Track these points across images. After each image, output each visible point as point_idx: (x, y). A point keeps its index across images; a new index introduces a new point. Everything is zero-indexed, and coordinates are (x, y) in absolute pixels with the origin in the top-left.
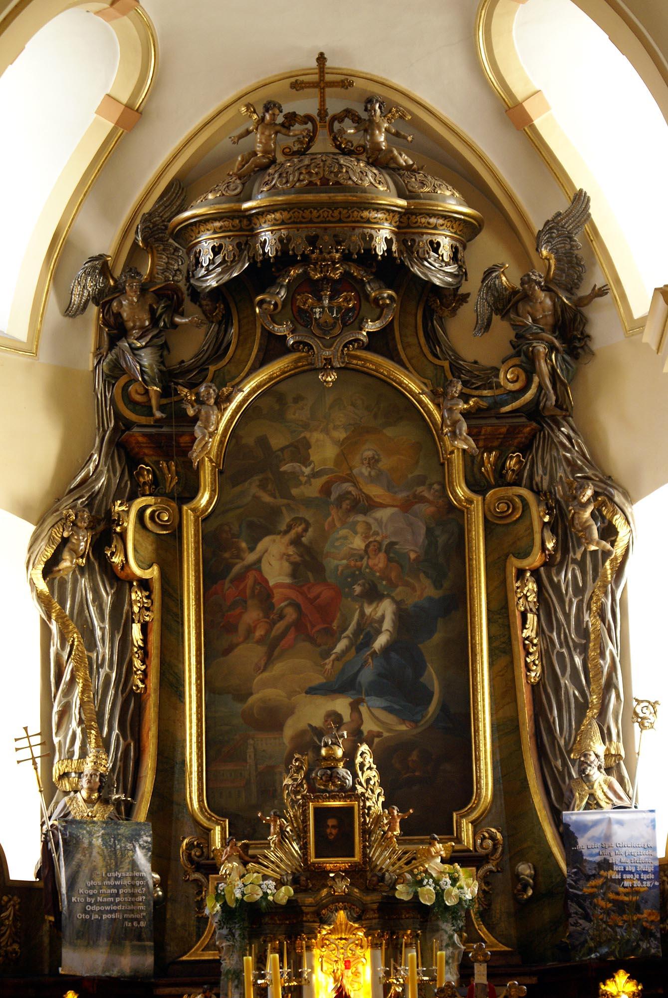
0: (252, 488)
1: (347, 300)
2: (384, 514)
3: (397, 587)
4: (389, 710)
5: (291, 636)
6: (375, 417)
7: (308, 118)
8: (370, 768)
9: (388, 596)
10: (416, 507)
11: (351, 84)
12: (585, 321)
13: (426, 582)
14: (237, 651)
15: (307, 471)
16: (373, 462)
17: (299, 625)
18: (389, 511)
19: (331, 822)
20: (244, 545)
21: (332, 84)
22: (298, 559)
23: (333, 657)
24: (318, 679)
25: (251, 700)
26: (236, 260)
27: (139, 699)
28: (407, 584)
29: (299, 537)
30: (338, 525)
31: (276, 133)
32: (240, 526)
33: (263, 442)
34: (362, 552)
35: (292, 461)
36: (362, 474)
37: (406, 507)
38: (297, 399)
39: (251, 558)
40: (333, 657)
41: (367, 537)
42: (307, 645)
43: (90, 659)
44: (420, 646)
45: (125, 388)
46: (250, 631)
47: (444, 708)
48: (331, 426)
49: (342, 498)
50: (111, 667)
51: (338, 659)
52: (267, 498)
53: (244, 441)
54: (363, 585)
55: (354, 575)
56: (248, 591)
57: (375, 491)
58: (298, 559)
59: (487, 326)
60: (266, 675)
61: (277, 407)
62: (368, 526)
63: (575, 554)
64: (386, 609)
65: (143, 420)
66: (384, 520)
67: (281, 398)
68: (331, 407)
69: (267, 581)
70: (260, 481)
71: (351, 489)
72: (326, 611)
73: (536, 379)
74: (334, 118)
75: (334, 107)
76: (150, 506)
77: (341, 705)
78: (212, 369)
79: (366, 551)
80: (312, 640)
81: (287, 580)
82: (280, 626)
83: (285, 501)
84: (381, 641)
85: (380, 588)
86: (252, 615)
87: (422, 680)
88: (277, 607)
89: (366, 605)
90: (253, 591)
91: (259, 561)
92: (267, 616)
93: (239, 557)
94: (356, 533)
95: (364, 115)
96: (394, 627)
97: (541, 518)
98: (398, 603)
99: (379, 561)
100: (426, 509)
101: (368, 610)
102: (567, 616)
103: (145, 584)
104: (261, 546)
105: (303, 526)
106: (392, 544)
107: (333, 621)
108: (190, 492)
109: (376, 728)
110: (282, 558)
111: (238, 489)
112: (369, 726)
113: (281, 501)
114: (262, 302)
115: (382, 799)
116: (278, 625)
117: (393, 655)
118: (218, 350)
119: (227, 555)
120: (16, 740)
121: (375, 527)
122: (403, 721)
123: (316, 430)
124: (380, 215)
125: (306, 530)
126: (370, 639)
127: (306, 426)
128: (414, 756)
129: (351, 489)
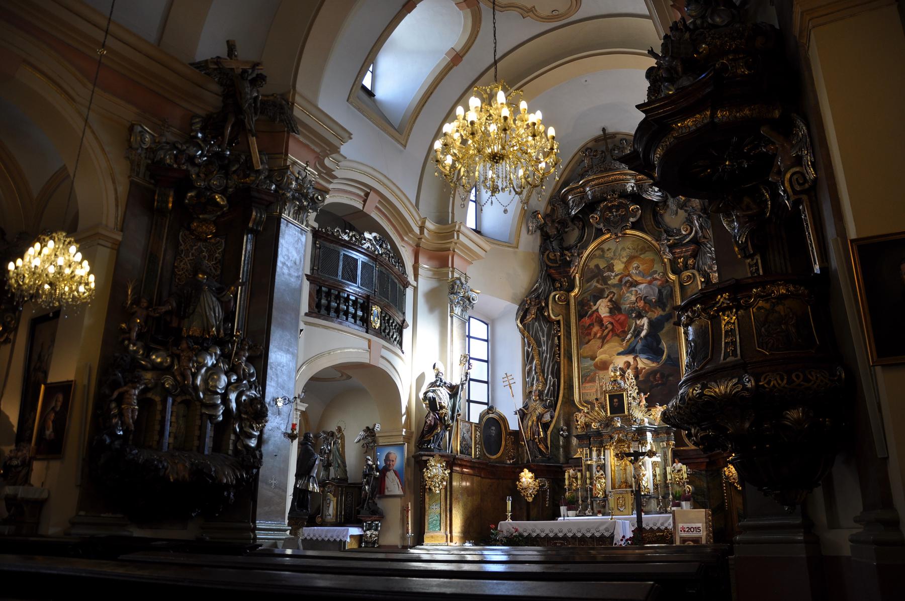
0: (594, 283)
1: (622, 212)
2: (642, 286)
3: (648, 312)
4: (648, 359)
5: (610, 334)
7: (603, 152)
8: (632, 379)
9: (646, 316)
11: (615, 137)
13: (660, 309)
14: (591, 343)
15: (613, 274)
17: (612, 330)
18: (644, 285)
19: (615, 400)
20: (592, 304)
21: (610, 138)
22: (611, 306)
24: (621, 350)
25: (596, 359)
26: (580, 203)
27: (559, 364)
29: (612, 298)
31: (592, 159)
33: (597, 266)
37: (650, 283)
38: (608, 250)
39: (594, 308)
42: (616, 337)
43: (539, 351)
44: (659, 334)
45: (548, 255)
46: (596, 334)
47: (669, 356)
49: (626, 282)
50: (547, 353)
51: (628, 341)
52: (599, 286)
55: (632, 310)
57: (639, 279)
58: (611, 306)
59: (677, 213)
60: (602, 349)
62: (637, 291)
64: (645, 321)
65: (555, 265)
67: (603, 250)
68: (621, 250)
72: (622, 324)
73: (694, 229)
74: (611, 150)
75: (610, 146)
76: (556, 295)
77: (630, 358)
78: (579, 245)
79: (636, 301)
80: (618, 335)
81: (608, 315)
82: (606, 331)
84: (643, 334)
85: (642, 314)
86: (596, 328)
87: (660, 346)
90: (596, 319)
91: (598, 309)
92: (601, 328)
95: (621, 146)
97: (701, 280)
98: (649, 319)
99: (641, 304)
100: (659, 283)
101: (638, 322)
103: (558, 322)
106: (646, 297)
108: (571, 288)
109: (643, 366)
111: (589, 284)
112: (640, 365)
113: (604, 286)
114: (592, 217)
115: (637, 391)
117: (648, 338)
118: (581, 237)
119: (586, 308)
121: (639, 292)
122: (653, 362)
124: (628, 177)
125: (614, 296)
126: (640, 332)
127: (612, 259)
128: (658, 375)
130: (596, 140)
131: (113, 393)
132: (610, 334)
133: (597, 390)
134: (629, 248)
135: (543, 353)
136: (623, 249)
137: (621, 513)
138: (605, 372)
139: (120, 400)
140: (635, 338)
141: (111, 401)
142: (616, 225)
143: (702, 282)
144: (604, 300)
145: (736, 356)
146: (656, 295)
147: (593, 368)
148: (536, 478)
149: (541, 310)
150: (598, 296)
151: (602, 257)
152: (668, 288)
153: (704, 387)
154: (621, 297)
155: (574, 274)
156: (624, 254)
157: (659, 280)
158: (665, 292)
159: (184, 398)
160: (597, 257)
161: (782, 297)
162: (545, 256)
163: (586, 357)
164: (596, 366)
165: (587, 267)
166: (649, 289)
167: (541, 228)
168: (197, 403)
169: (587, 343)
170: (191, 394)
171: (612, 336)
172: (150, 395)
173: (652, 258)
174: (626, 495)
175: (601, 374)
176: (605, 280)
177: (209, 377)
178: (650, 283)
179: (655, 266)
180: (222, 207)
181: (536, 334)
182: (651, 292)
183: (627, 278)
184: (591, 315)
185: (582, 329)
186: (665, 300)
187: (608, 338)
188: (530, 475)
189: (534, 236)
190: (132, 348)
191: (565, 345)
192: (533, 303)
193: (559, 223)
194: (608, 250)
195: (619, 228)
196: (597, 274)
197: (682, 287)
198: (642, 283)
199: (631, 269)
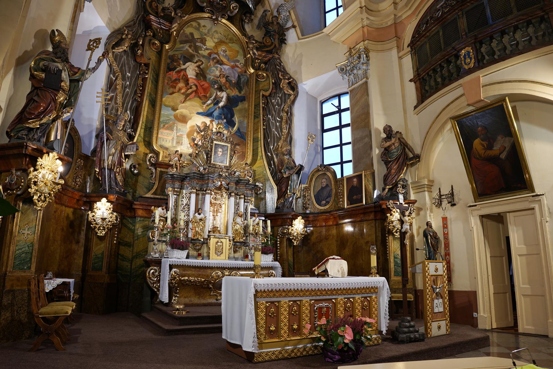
0: (187, 47)
2: (226, 67)
3: (228, 89)
5: (194, 94)
6: (227, 39)
9: (225, 91)
10: (236, 68)
12: (285, 35)
13: (237, 91)
14: (174, 95)
15: (205, 47)
16: (225, 51)
17: (196, 92)
20: (181, 62)
22: (198, 72)
23: (206, 105)
25: (177, 111)
28: (231, 89)
30: (212, 66)
32: (181, 57)
33: (192, 34)
34: (219, 76)
35: (200, 43)
36: (221, 54)
37: (233, 67)
39: (183, 67)
40: (206, 105)
41: (220, 72)
46: (180, 89)
47: (239, 129)
48: (213, 37)
51: (207, 106)
52: (191, 51)
53: (186, 32)
54: (218, 86)
55: (216, 82)
56: (181, 77)
57: (224, 60)
58: (198, 72)
60: (183, 104)
61: (197, 26)
62: (221, 69)
63: (279, 95)
64: (224, 95)
66: (226, 69)
67: (199, 24)
68: (214, 32)
69: (187, 76)
70: (189, 45)
71: (217, 57)
72: (205, 90)
77: (207, 120)
79: (220, 76)
80: (200, 98)
81: (194, 77)
82: (190, 91)
83: (197, 54)
84: (221, 104)
85: (223, 88)
86: (181, 85)
87: (233, 119)
88: (190, 85)
89: (218, 92)
90: (183, 77)
91: (186, 69)
92: (186, 86)
93: (179, 65)
94: (217, 70)
96: (226, 101)
98: (228, 94)
99: (223, 80)
100: (240, 70)
101: (219, 93)
104: (187, 64)
105: (201, 63)
106: (227, 77)
107: (207, 94)
110: (193, 70)
111: (182, 45)
113: (195, 53)
116: (189, 90)
117: (225, 109)
119: (175, 64)
120: (98, 93)
121: (223, 70)
123: (209, 37)
125: (202, 64)
127: (206, 35)
129: (217, 57)
132: (194, 94)
133: (173, 138)
134: (220, 34)
135: (125, 88)
136: (216, 32)
137: (219, 257)
138: (184, 124)
140: (214, 105)
143: (273, 83)
144: (193, 64)
146: (236, 78)
147: (173, 117)
148: (114, 211)
149: (134, 47)
150: (188, 58)
151: (198, 29)
152: (245, 77)
154: (208, 67)
155: (173, 30)
157: (240, 68)
158: (242, 80)
160: (193, 28)
164: (176, 117)
165: (182, 31)
166: (231, 72)
169: (171, 94)
171: (195, 96)
173: (237, 50)
175: (180, 125)
176: (197, 49)
179: (238, 56)
181: (122, 67)
182: (233, 75)
183: (215, 56)
184: (179, 72)
185: (168, 80)
186: (242, 85)
187: (191, 96)
191: (149, 88)
192: (129, 36)
194: (204, 26)
195: (221, 14)
196: (190, 40)
198: (227, 65)
199: (219, 50)
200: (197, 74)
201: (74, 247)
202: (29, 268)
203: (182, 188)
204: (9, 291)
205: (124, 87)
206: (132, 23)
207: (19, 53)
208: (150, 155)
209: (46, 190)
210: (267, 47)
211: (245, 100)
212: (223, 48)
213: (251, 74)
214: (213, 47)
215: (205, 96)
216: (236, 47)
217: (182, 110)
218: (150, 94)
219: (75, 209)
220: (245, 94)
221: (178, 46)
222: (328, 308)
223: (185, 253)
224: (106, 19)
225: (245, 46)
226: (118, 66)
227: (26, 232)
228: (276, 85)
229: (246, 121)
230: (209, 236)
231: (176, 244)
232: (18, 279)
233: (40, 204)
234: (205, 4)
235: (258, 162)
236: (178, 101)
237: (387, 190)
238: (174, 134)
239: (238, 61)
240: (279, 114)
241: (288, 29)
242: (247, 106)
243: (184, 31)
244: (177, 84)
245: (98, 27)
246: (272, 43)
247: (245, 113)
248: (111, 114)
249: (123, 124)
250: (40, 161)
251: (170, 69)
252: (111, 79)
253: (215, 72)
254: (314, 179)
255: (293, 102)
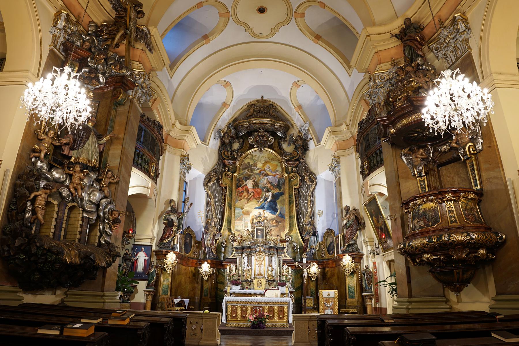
0: (246, 171)
1: (265, 139)
2: (270, 177)
5: (252, 197)
12: (308, 145)
13: (278, 189)
15: (257, 168)
17: (253, 196)
19: (259, 231)
33: (249, 163)
37: (274, 176)
39: (245, 183)
45: (224, 153)
46: (244, 197)
47: (280, 213)
52: (249, 173)
55: (264, 188)
57: (269, 173)
64: (270, 194)
67: (252, 156)
72: (259, 194)
77: (261, 211)
80: (256, 199)
81: (252, 188)
82: (250, 196)
84: (269, 200)
86: (245, 194)
98: (272, 193)
99: (269, 185)
100: (279, 176)
101: (267, 194)
102: (304, 197)
106: (272, 182)
113: (251, 174)
127: (257, 161)
128: (274, 221)
130: (258, 101)
131: (30, 194)
132: (252, 197)
135: (216, 202)
136: (263, 157)
138: (248, 216)
139: (34, 201)
141: (28, 201)
142: (261, 144)
143: (300, 180)
145: (457, 223)
147: (241, 213)
148: (211, 267)
149: (218, 180)
150: (247, 178)
151: (252, 159)
153: (449, 236)
154: (259, 180)
156: (263, 159)
158: (281, 182)
159: (73, 204)
161: (471, 199)
162: (222, 153)
163: (237, 207)
164: (243, 213)
167: (221, 139)
168: (81, 209)
169: (240, 200)
170: (78, 203)
171: (253, 199)
172: (50, 199)
174: (262, 280)
175: (246, 217)
176: (252, 171)
177: (91, 192)
178: (274, 176)
180: (100, 83)
182: (275, 181)
184: (243, 187)
186: (281, 185)
188: (208, 265)
189: (217, 141)
190: (39, 164)
192: (214, 176)
193: (231, 137)
194: (255, 156)
195: (263, 146)
196: (248, 167)
197: (290, 180)
199: (265, 167)
200: (253, 185)
201: (196, 285)
202: (168, 294)
203: (242, 253)
204: (161, 302)
205: (215, 203)
206: (216, 167)
207: (159, 213)
208: (231, 236)
209: (170, 266)
210: (294, 157)
211: (283, 194)
212: (268, 165)
213: (286, 177)
214: (262, 167)
215: (259, 197)
216: (276, 162)
217: (247, 208)
218: (229, 203)
219: (195, 267)
220: (283, 190)
221: (242, 172)
222: (259, 309)
223: (239, 287)
224: (202, 170)
225: (281, 160)
226: (211, 192)
227: (166, 281)
228: (302, 180)
229: (285, 207)
230: (254, 278)
231: (235, 283)
232: (164, 298)
233: (169, 271)
234: (254, 143)
235: (294, 230)
236: (244, 203)
237: (345, 247)
238: (243, 222)
239: (277, 171)
240: (306, 198)
241: (308, 141)
242: (285, 197)
243: (244, 162)
244: (243, 194)
245: (200, 175)
246: (298, 154)
247: (283, 202)
248: (209, 218)
249: (213, 223)
250: (167, 256)
251: (238, 186)
252: (208, 200)
253: (263, 181)
254: (326, 238)
255: (314, 189)
